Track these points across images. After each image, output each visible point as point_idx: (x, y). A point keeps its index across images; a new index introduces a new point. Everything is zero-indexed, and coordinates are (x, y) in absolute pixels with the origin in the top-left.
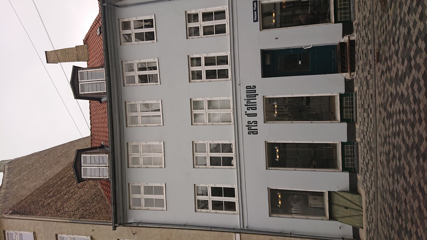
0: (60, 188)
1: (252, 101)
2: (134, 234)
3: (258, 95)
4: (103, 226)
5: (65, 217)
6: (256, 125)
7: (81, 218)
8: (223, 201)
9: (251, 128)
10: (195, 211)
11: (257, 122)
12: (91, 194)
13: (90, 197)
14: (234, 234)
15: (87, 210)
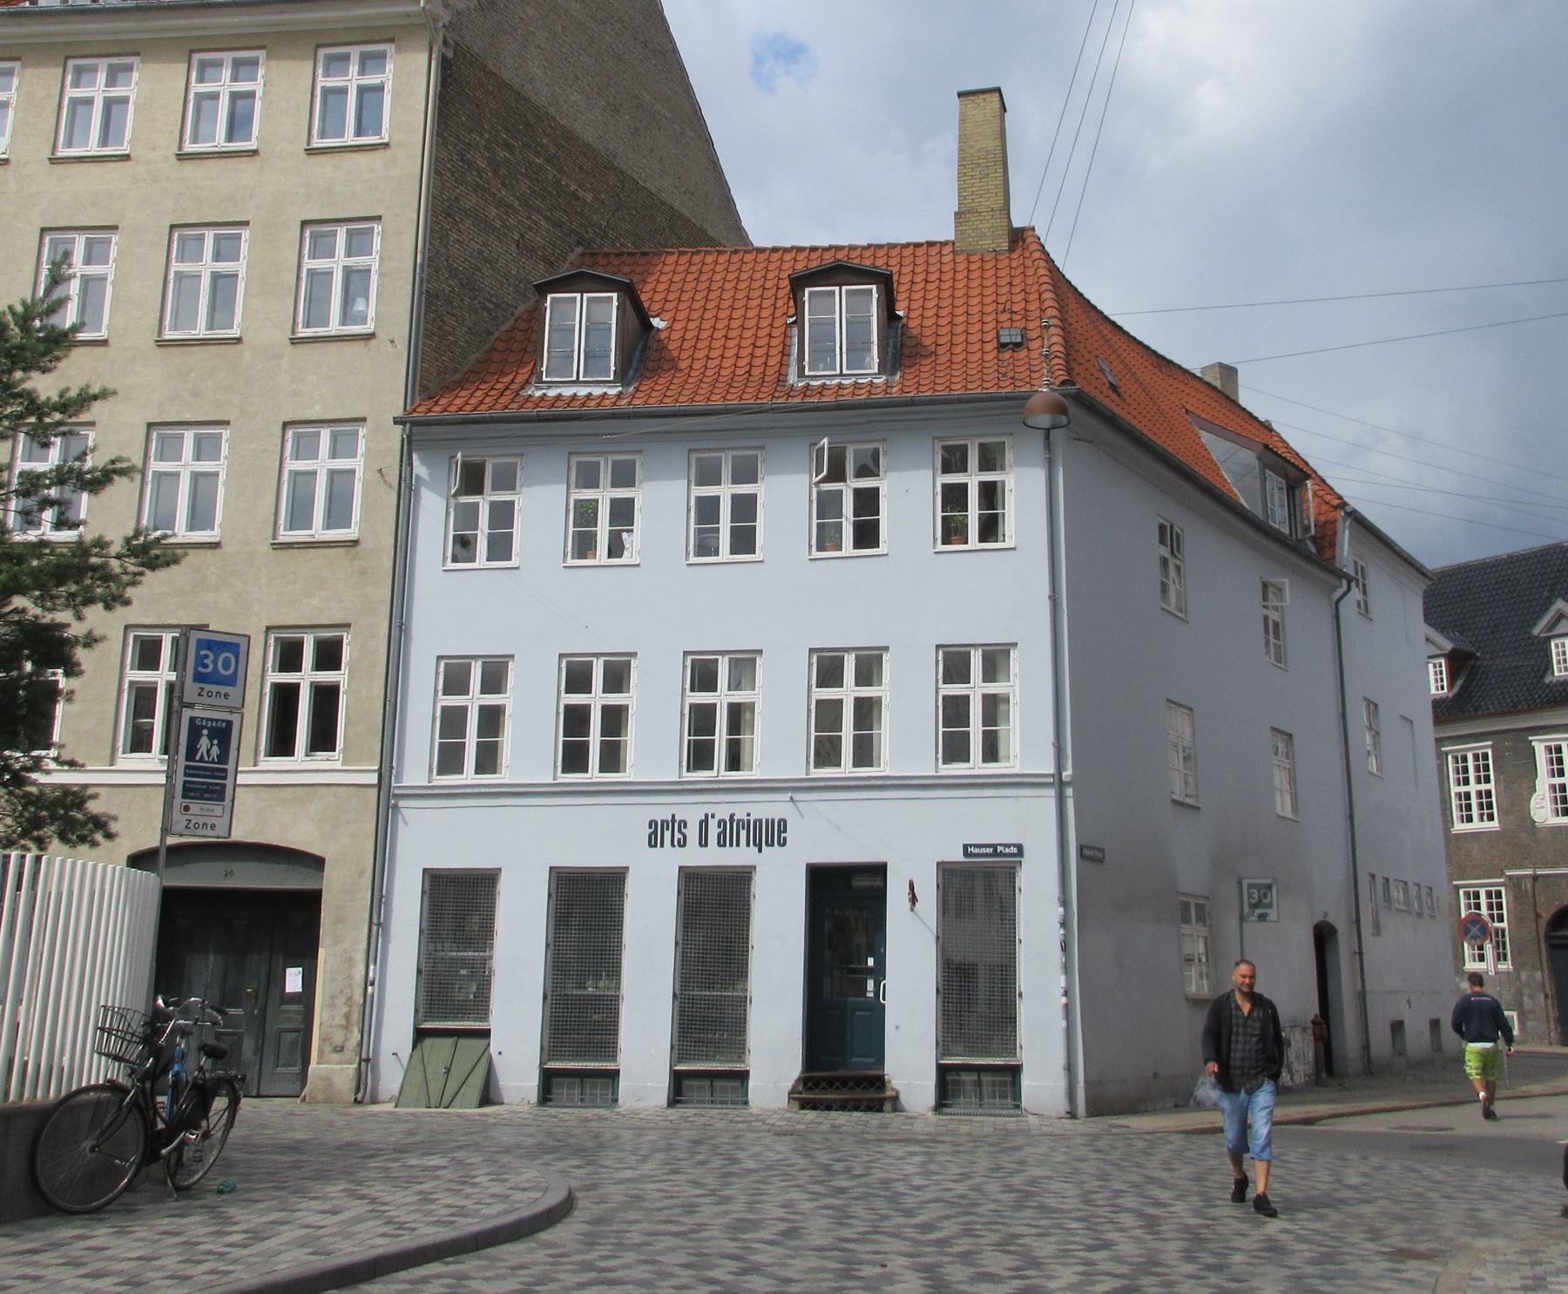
0: (521, 173)
1: (743, 834)
2: (380, 471)
3: (760, 851)
6: (676, 843)
7: (427, 299)
8: (467, 740)
9: (668, 829)
11: (685, 845)
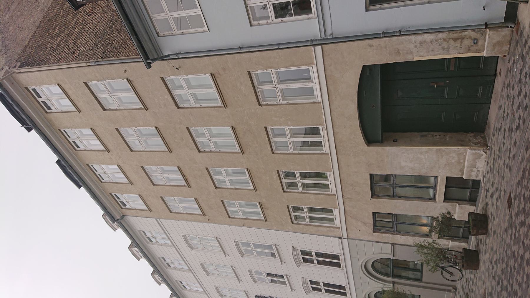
4: (135, 64)
5: (83, 60)
10: (251, 26)
12: (106, 20)
13: (106, 26)
14: (313, 48)
15: (108, 44)
